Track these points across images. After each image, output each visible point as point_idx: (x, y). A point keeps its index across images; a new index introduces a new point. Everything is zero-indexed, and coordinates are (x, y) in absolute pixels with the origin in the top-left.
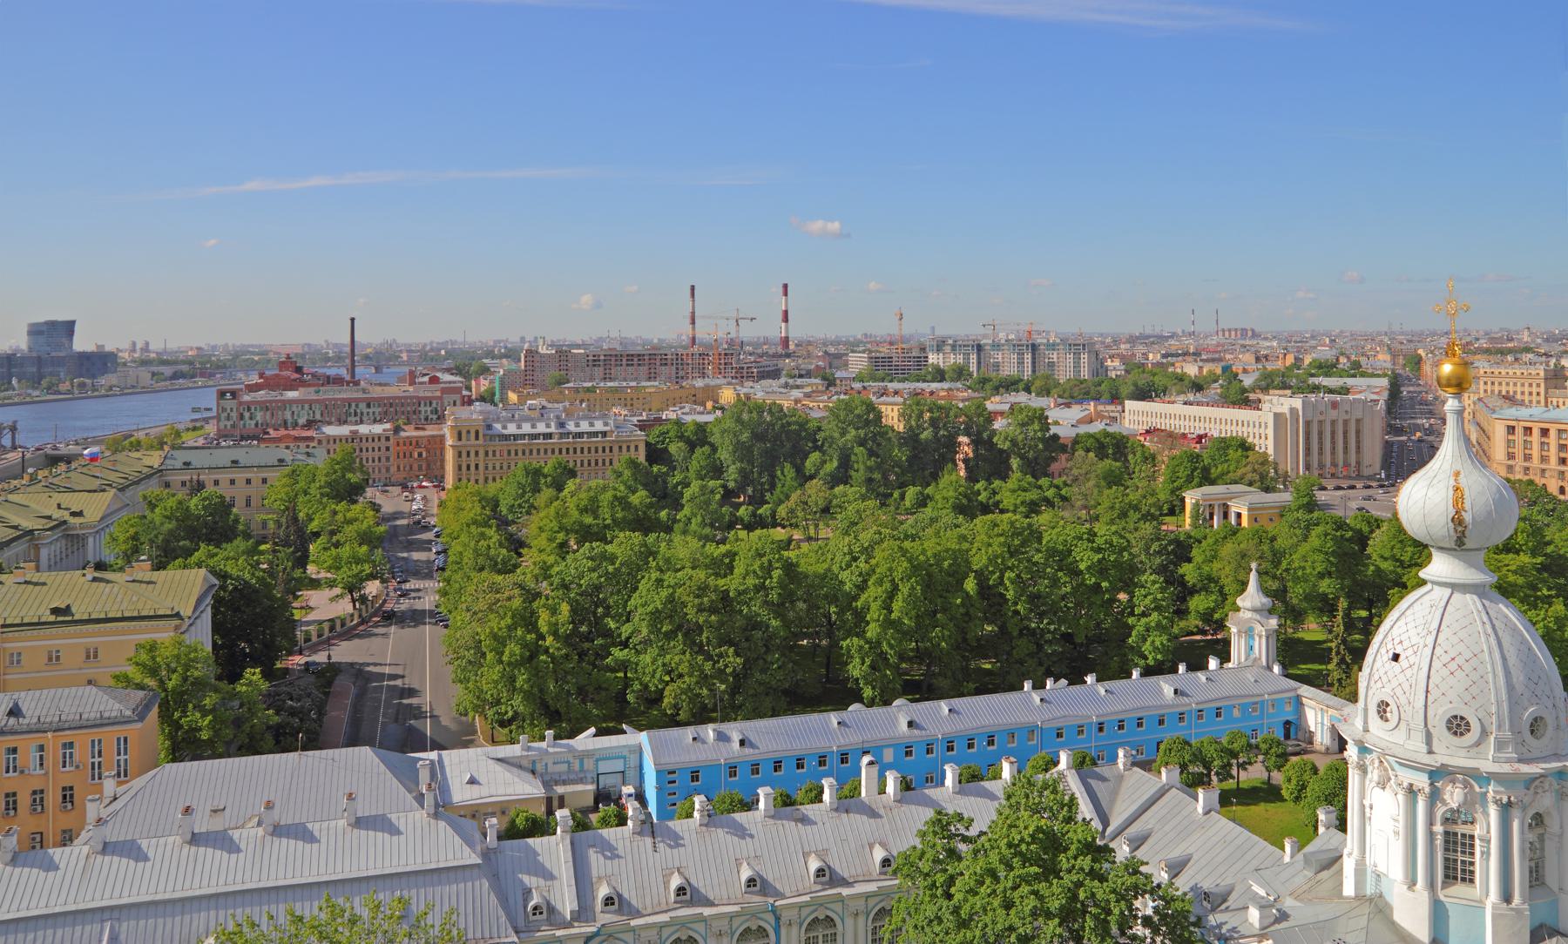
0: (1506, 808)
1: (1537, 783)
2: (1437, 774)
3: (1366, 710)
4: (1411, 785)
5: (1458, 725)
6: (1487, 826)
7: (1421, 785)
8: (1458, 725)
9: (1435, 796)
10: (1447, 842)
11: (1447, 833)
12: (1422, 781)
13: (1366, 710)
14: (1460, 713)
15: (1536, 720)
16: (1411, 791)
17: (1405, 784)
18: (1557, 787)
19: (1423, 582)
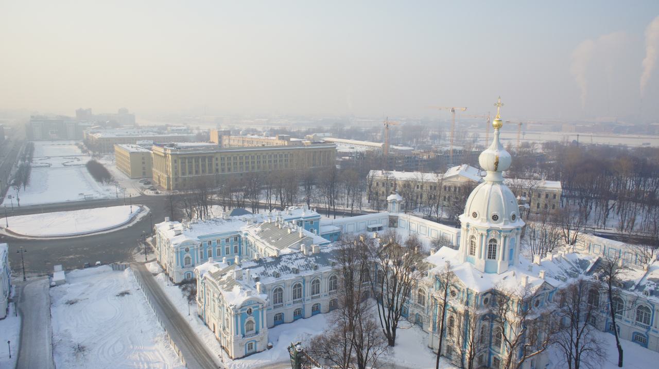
0: (505, 238)
5: (495, 218)
6: (500, 242)
8: (495, 218)
9: (487, 237)
10: (489, 248)
11: (490, 245)
16: (482, 235)
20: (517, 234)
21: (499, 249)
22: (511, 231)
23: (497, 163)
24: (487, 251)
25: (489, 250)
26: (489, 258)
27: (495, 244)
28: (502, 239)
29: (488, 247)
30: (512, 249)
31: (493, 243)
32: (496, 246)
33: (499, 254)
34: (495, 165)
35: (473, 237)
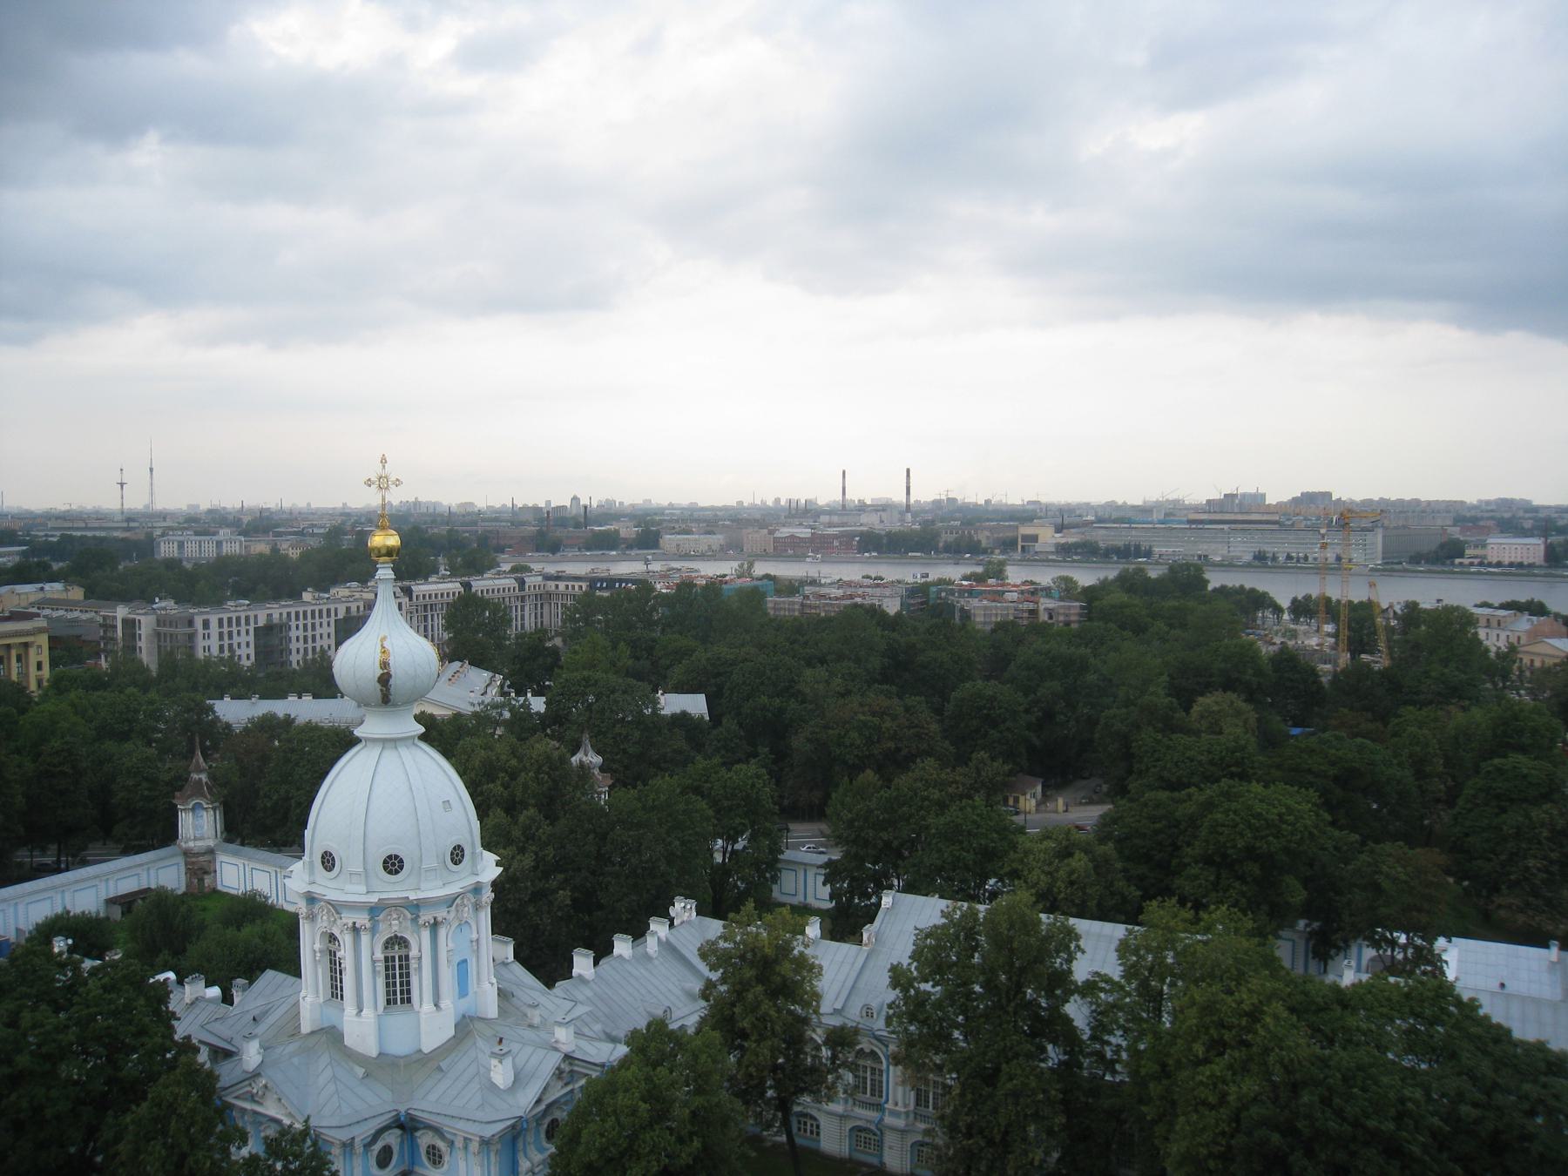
1: (458, 901)
2: (374, 910)
3: (311, 863)
4: (354, 923)
6: (420, 944)
7: (363, 922)
8: (393, 865)
10: (387, 968)
11: (386, 959)
12: (362, 919)
13: (311, 863)
14: (394, 853)
15: (454, 848)
16: (355, 930)
17: (350, 925)
18: (473, 900)
19: (357, 741)
20: (477, 907)
21: (420, 968)
22: (450, 901)
23: (385, 680)
24: (381, 981)
25: (387, 977)
26: (388, 1002)
27: (403, 952)
28: (426, 935)
29: (381, 966)
30: (465, 961)
31: (396, 952)
32: (407, 957)
33: (421, 984)
34: (378, 687)
35: (332, 938)
